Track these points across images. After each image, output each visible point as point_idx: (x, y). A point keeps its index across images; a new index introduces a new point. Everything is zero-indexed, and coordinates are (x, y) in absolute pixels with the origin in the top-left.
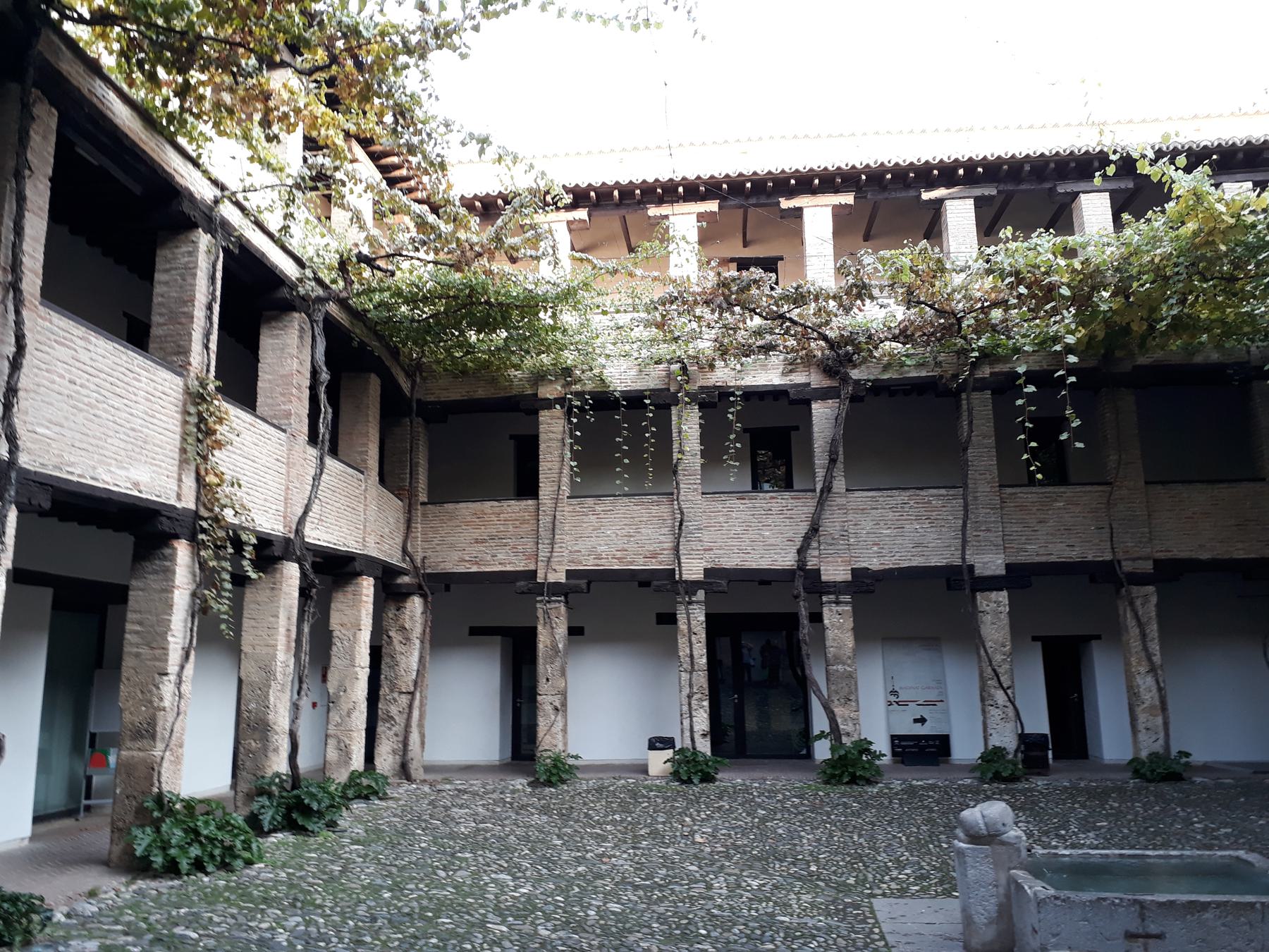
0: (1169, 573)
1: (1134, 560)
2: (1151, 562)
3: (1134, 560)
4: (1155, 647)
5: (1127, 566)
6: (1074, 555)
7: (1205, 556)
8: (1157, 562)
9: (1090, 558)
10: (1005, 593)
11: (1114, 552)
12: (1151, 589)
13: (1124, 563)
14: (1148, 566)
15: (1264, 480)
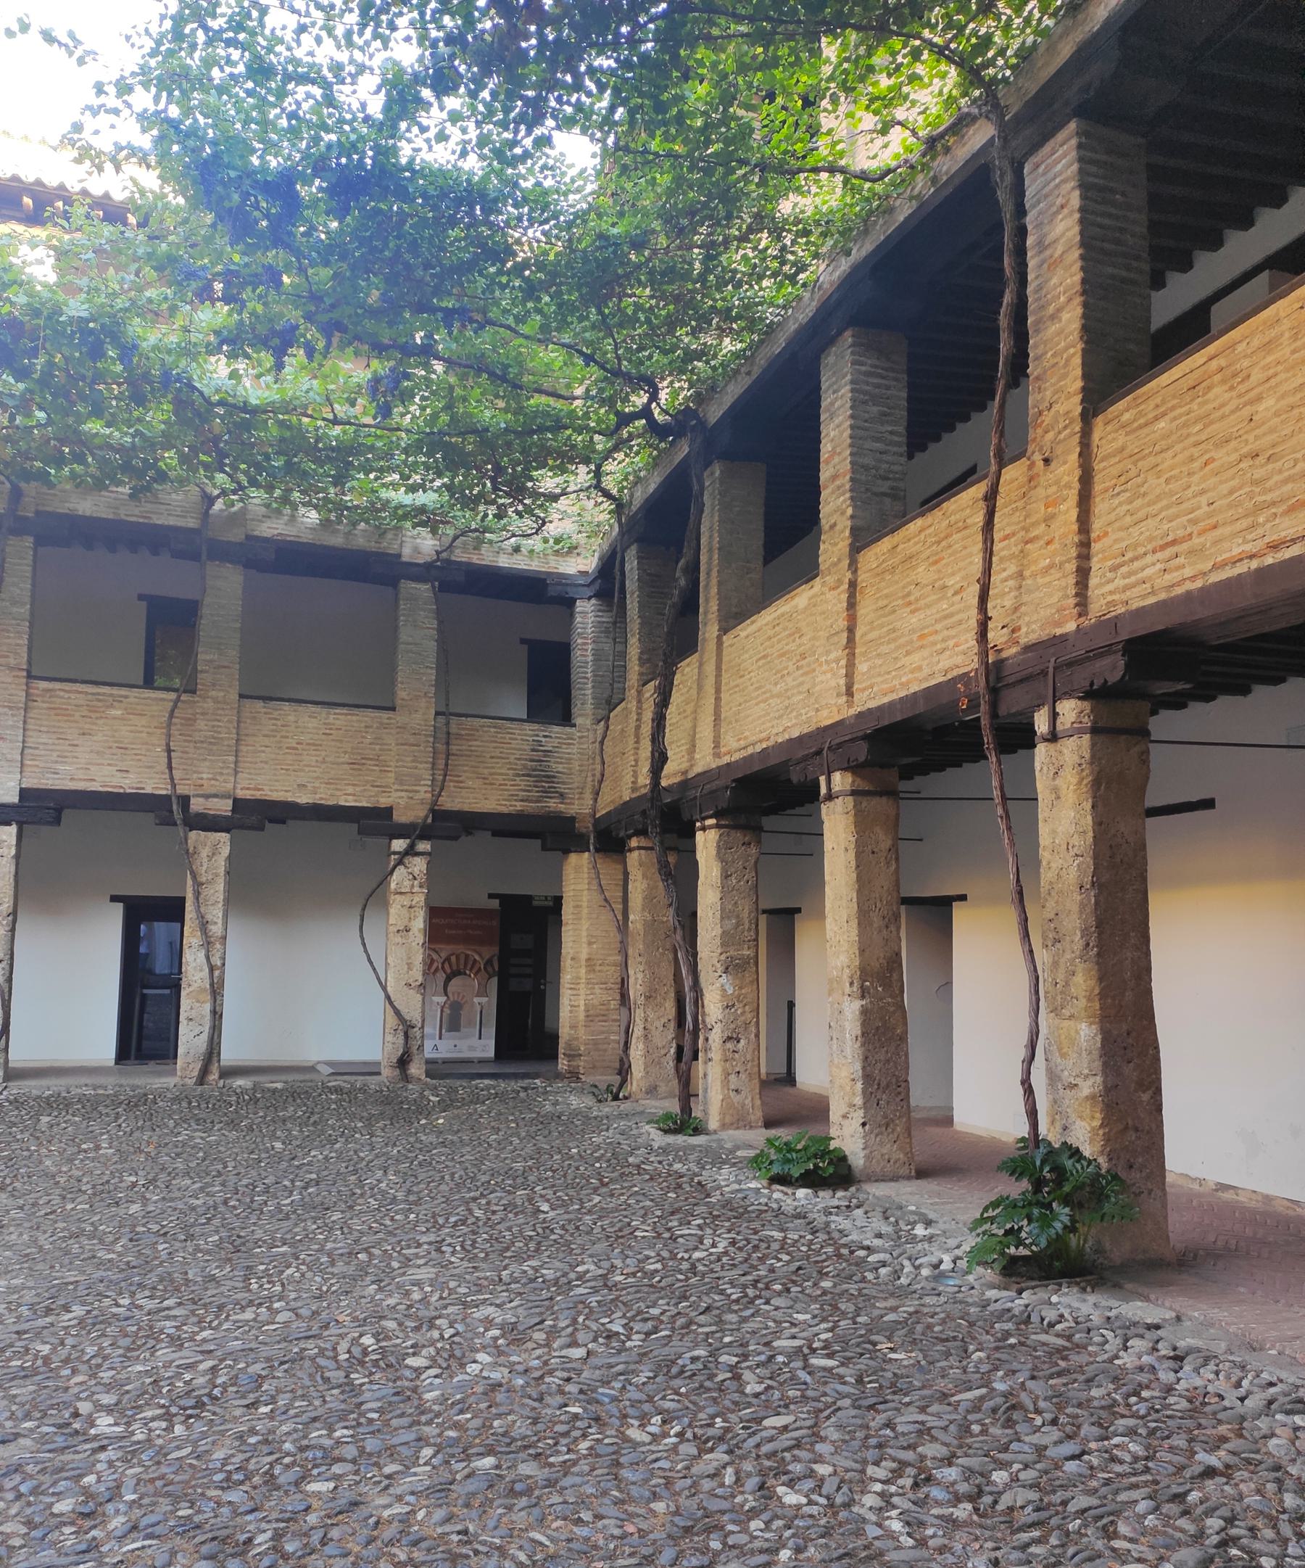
0: (254, 817)
1: (207, 797)
2: (230, 802)
3: (207, 797)
4: (215, 913)
5: (197, 805)
6: (127, 783)
7: (303, 799)
8: (238, 804)
9: (148, 790)
10: (13, 829)
11: (174, 786)
12: (224, 837)
13: (193, 801)
14: (223, 807)
15: (393, 709)
